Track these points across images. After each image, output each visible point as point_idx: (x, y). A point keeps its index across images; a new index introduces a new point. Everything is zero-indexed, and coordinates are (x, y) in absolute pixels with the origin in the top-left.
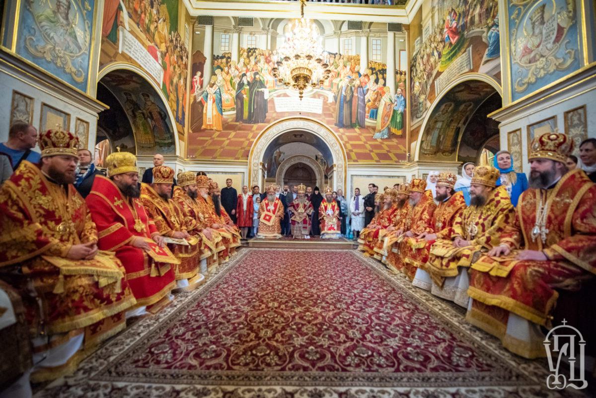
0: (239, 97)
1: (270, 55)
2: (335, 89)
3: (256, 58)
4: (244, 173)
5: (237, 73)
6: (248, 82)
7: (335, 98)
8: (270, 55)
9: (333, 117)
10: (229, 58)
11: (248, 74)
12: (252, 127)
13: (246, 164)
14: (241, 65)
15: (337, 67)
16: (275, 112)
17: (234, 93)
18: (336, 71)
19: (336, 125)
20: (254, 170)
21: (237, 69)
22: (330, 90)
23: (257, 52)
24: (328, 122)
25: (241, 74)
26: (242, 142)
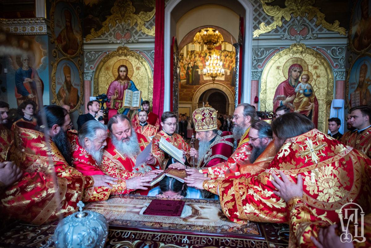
0: (187, 74)
1: (201, 53)
2: (230, 68)
3: (195, 55)
4: (190, 107)
5: (186, 62)
6: (191, 66)
7: (231, 73)
8: (201, 53)
9: (229, 81)
10: (183, 55)
11: (191, 63)
12: (193, 87)
13: (191, 104)
14: (188, 59)
15: (231, 58)
16: (203, 80)
17: (185, 72)
18: (231, 60)
19: (231, 85)
20: (195, 106)
21: (186, 60)
22: (228, 69)
23: (195, 52)
24: (227, 84)
25: (188, 63)
26: (189, 94)
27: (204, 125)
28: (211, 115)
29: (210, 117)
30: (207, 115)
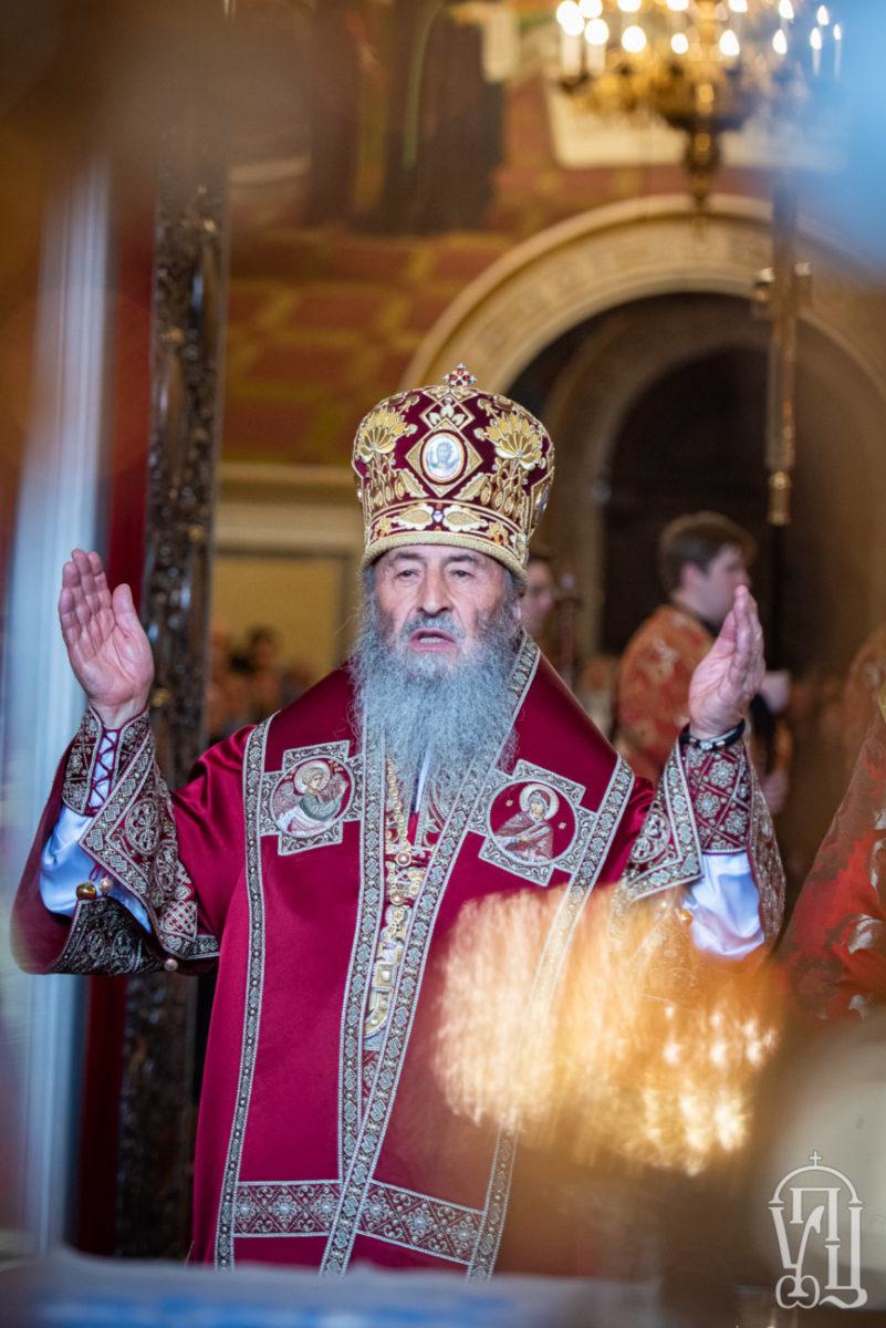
12: (403, 260)
27: (407, 497)
28: (482, 420)
29: (468, 431)
30: (448, 410)
